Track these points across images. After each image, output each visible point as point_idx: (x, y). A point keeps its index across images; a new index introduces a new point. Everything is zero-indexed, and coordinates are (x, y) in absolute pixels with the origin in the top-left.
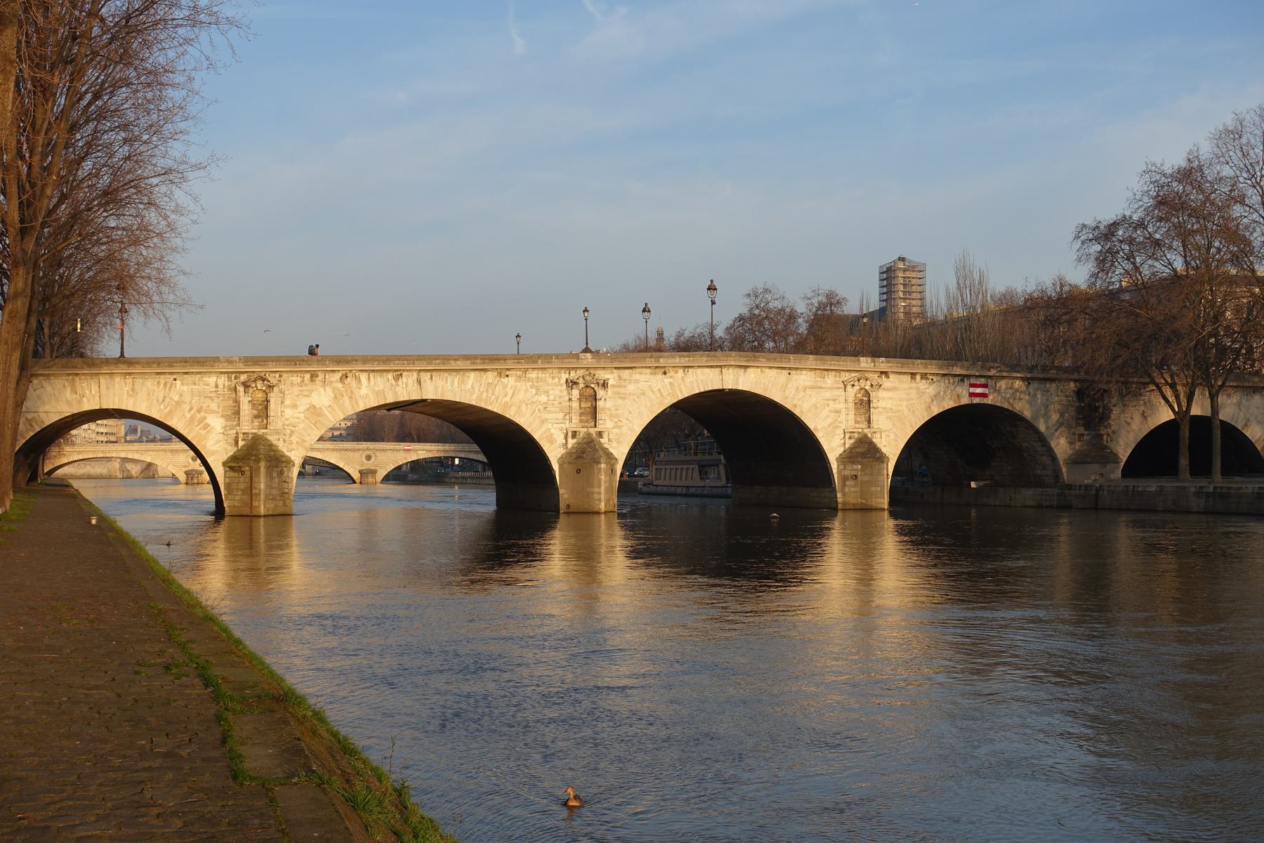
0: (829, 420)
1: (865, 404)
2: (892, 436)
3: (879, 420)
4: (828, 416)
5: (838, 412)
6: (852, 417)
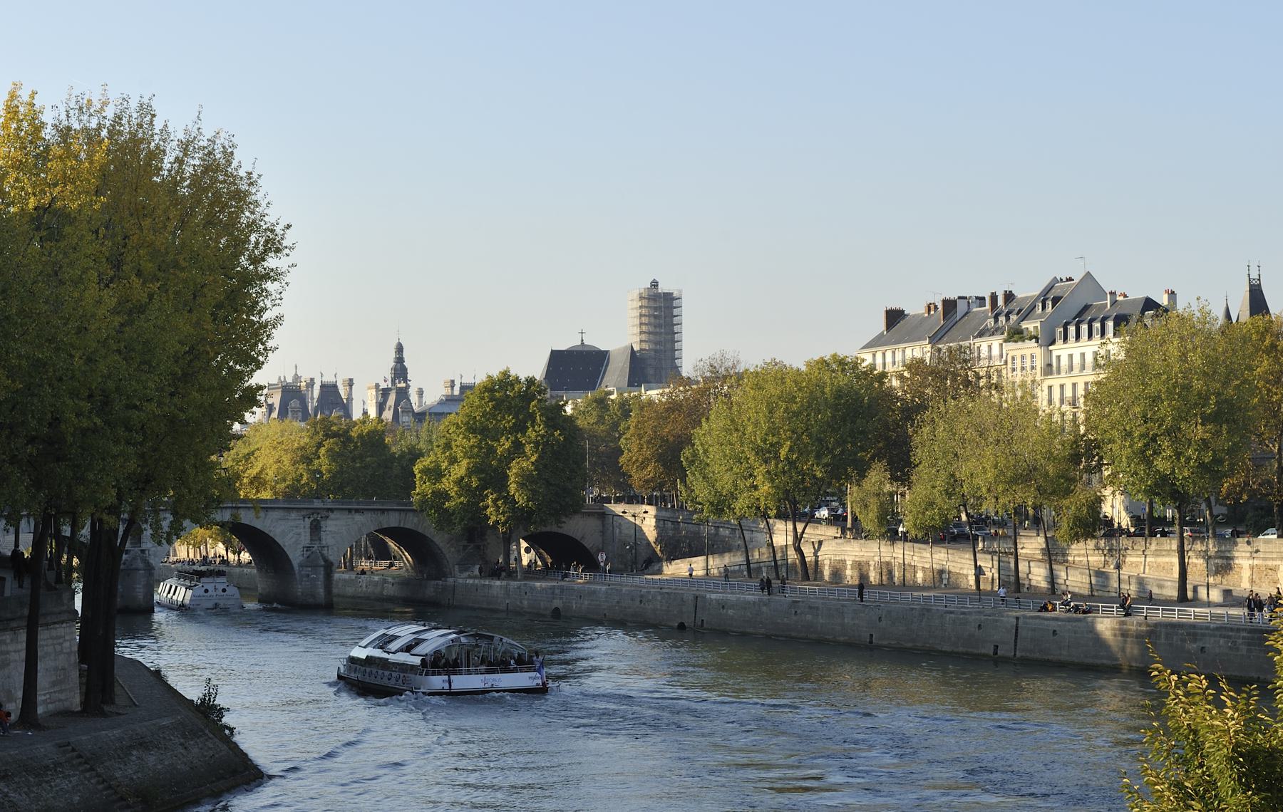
0: (293, 540)
1: (316, 529)
2: (336, 549)
3: (327, 539)
4: (292, 538)
5: (299, 534)
6: (308, 538)
